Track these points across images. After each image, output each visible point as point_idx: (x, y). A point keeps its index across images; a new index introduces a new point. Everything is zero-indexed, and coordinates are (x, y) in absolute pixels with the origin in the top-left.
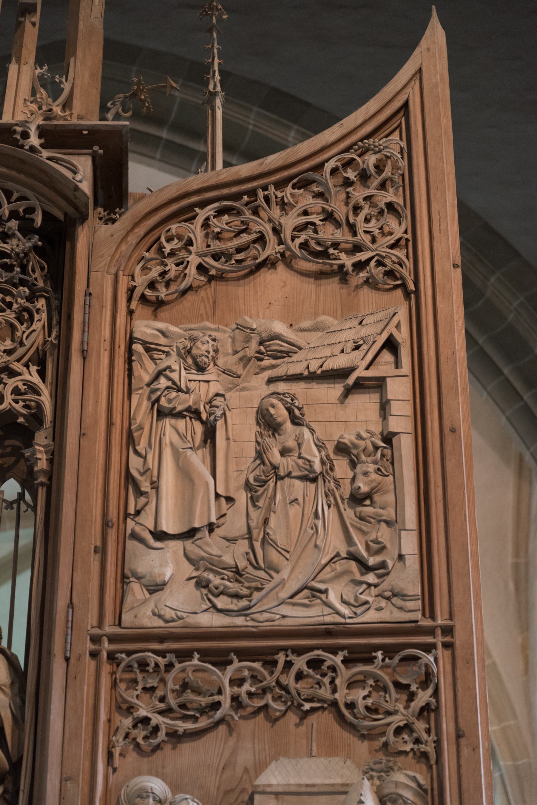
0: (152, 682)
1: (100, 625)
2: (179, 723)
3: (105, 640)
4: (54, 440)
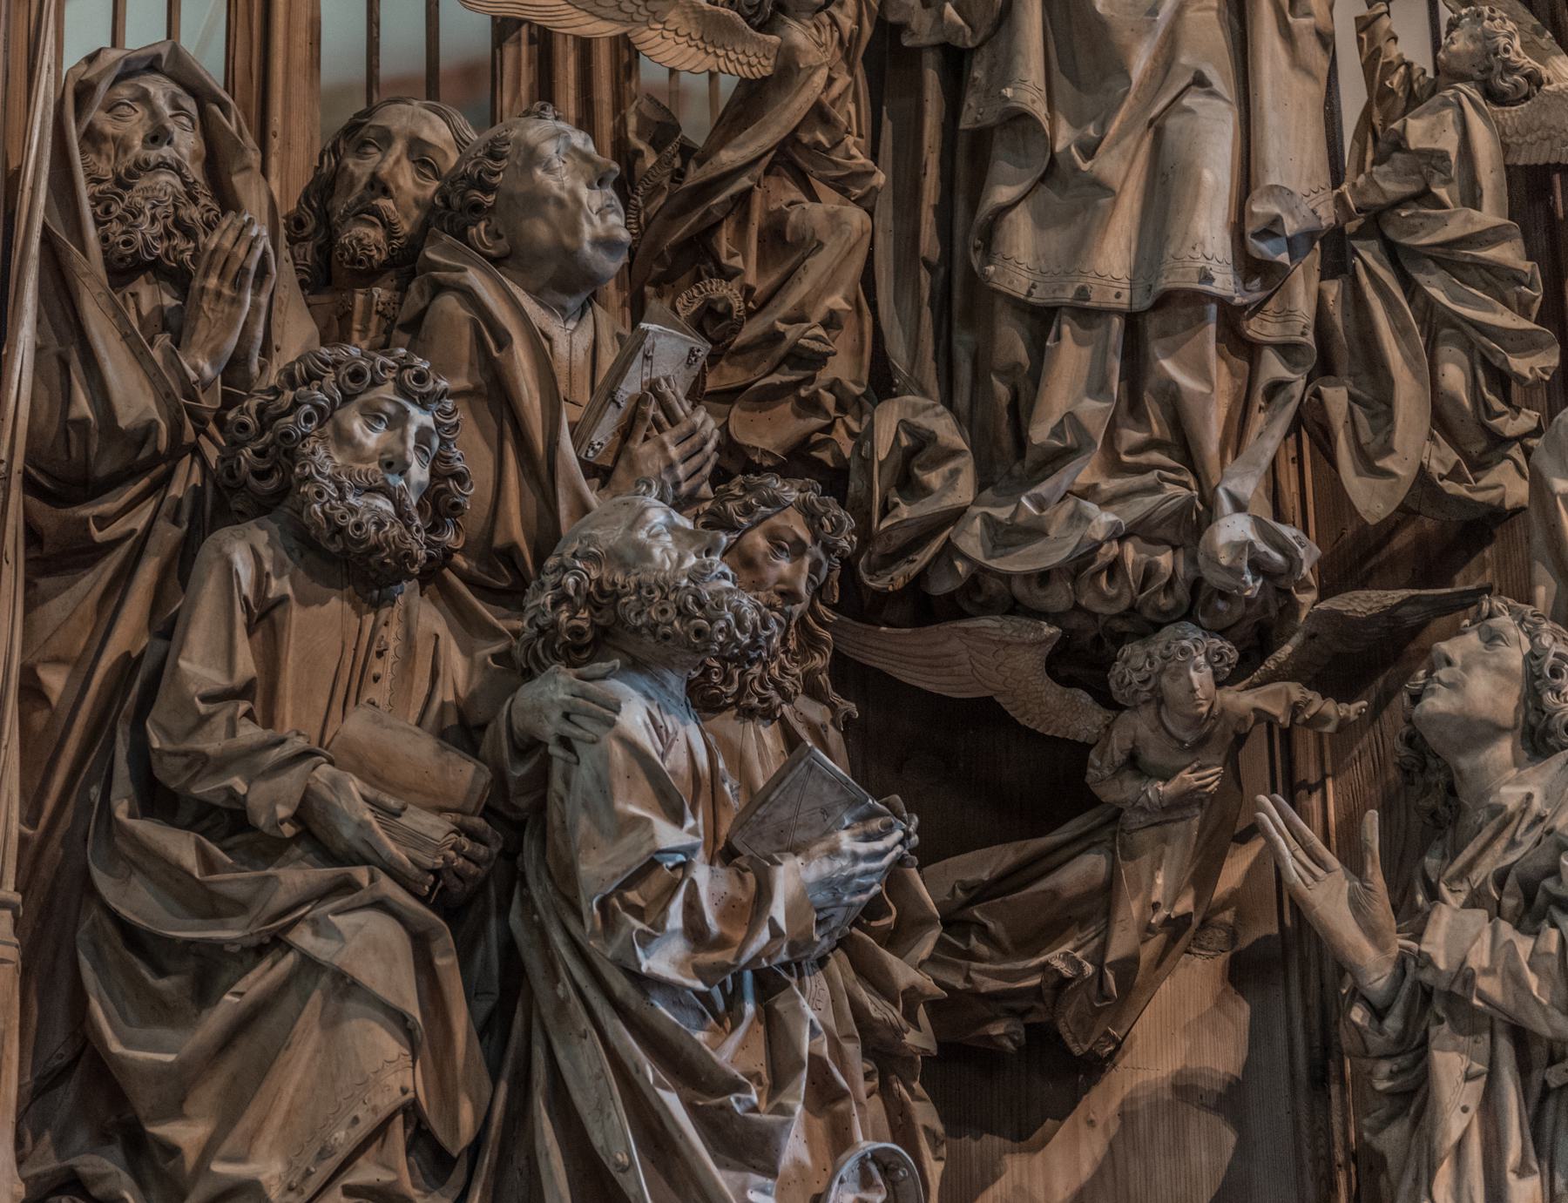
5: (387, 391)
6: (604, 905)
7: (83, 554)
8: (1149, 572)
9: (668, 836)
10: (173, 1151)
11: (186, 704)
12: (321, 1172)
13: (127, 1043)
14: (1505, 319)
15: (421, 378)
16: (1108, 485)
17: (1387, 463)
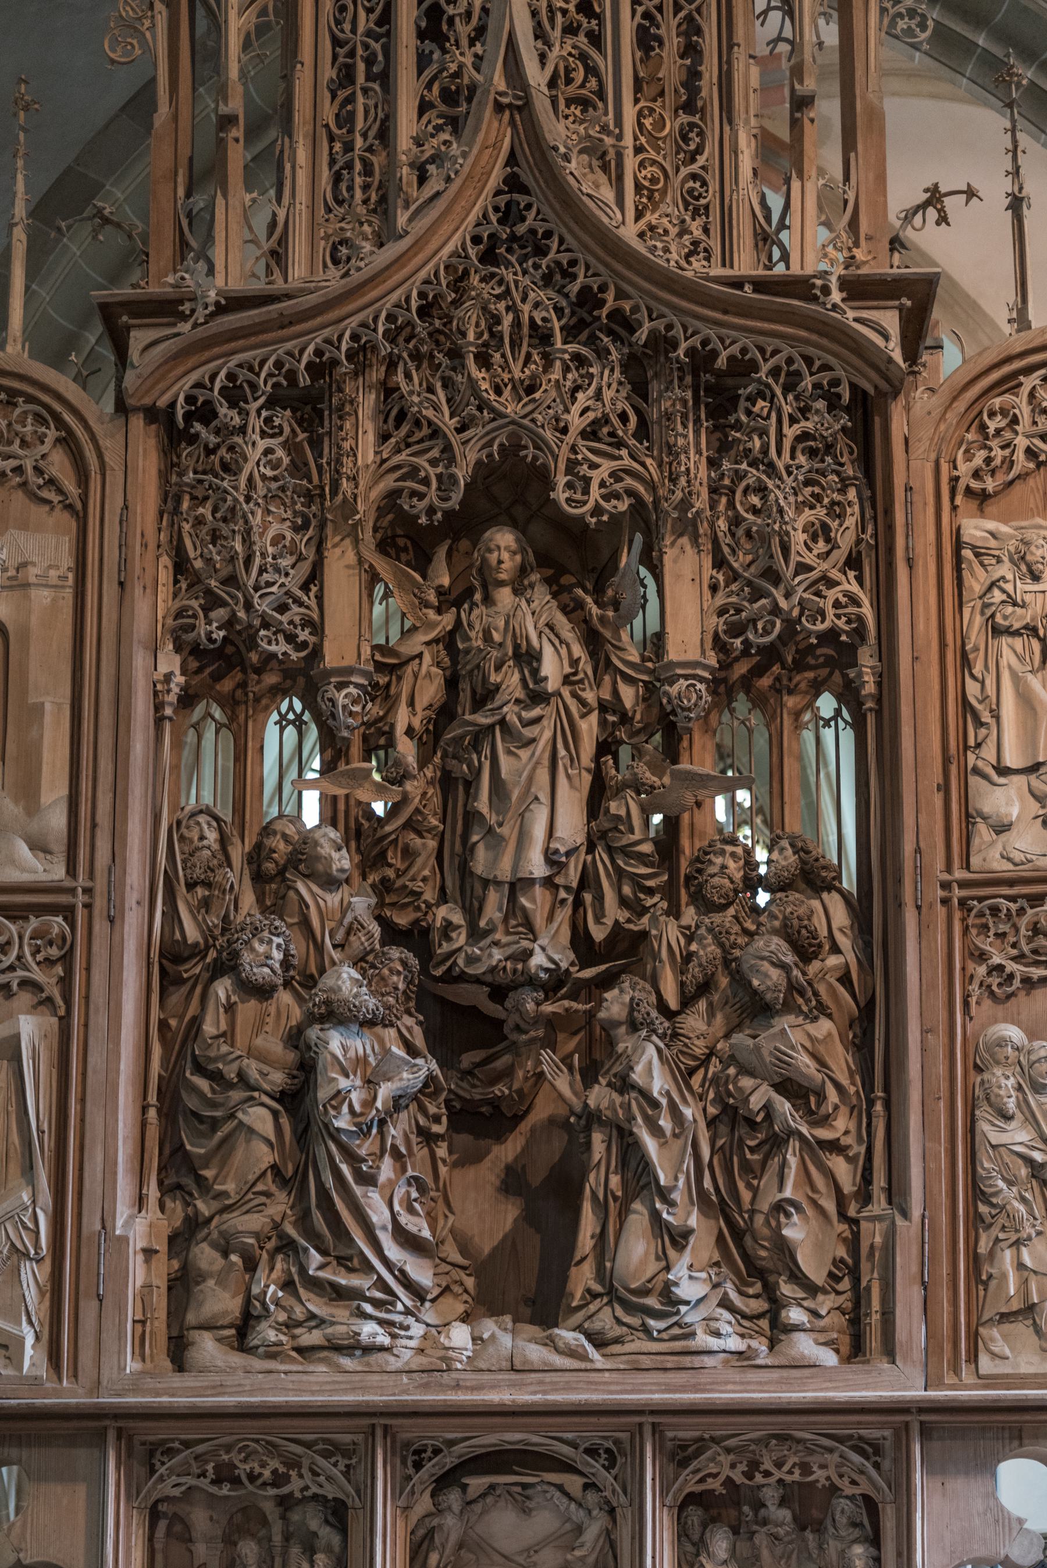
0: (1003, 928)
1: (949, 869)
2: (1032, 969)
3: (955, 885)
4: (880, 660)
5: (266, 934)
6: (324, 1106)
7: (180, 981)
8: (515, 971)
9: (343, 1083)
10: (206, 1179)
11: (205, 1040)
12: (245, 1189)
13: (192, 1145)
14: (643, 870)
15: (276, 928)
16: (505, 939)
17: (604, 920)
